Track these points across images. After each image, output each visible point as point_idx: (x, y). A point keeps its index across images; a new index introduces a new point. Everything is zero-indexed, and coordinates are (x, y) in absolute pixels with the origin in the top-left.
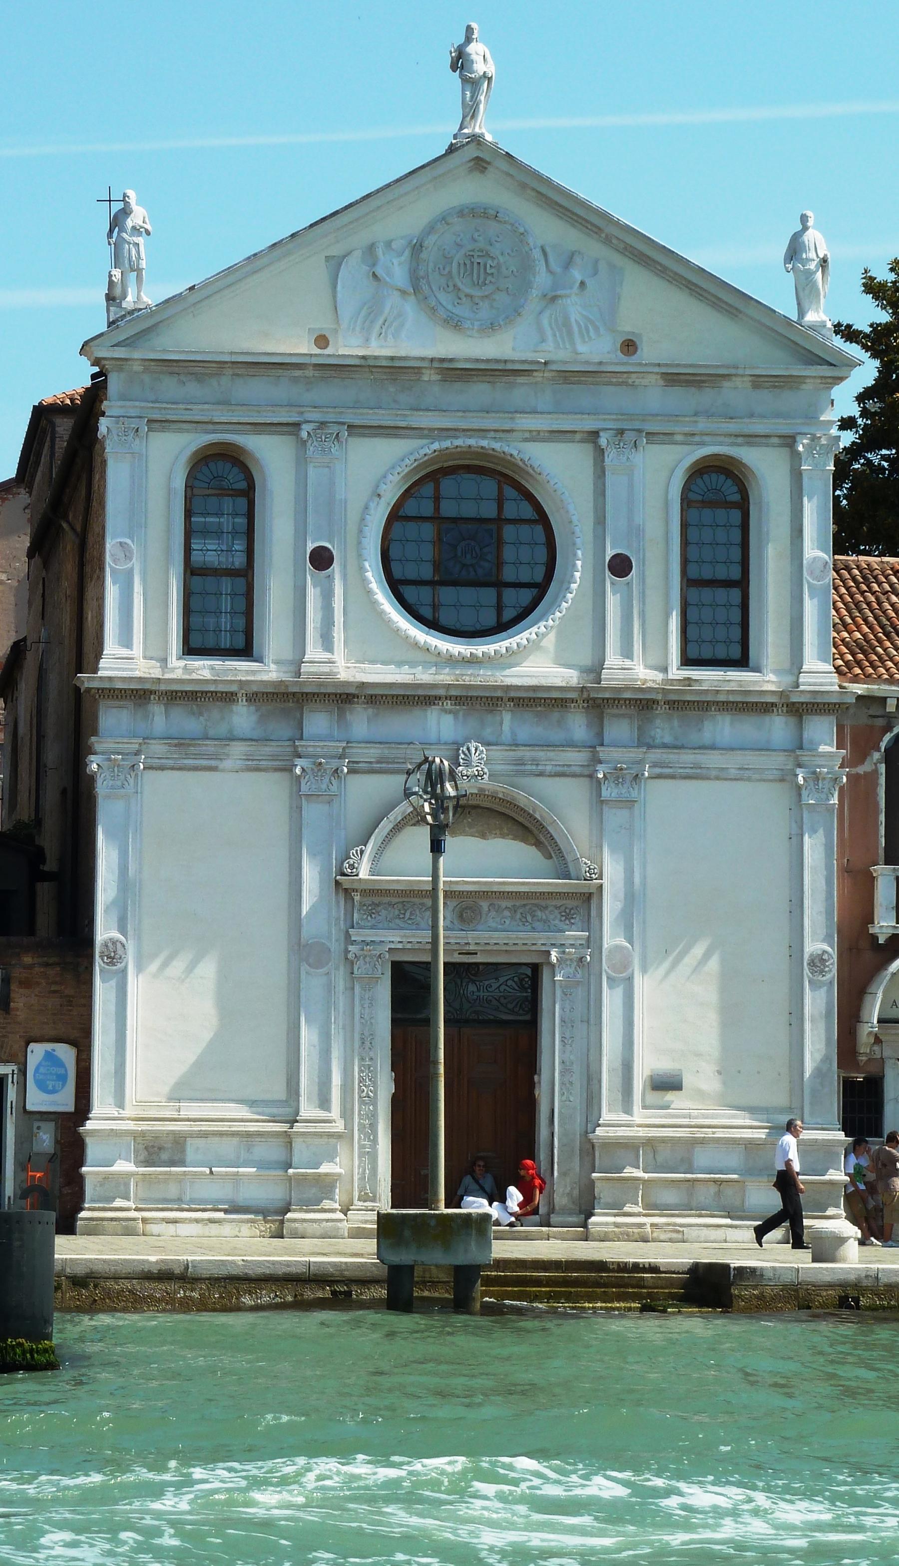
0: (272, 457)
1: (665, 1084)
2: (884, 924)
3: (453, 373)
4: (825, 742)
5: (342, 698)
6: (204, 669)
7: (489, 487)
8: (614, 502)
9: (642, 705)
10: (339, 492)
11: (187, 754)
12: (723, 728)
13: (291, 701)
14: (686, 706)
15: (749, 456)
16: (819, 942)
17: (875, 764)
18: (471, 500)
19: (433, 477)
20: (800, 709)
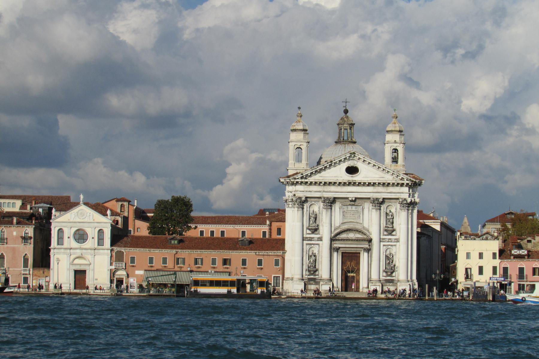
1: (97, 280)
6: (59, 246)
8: (92, 233)
12: (101, 251)
17: (114, 254)
18: (81, 232)
19: (78, 230)
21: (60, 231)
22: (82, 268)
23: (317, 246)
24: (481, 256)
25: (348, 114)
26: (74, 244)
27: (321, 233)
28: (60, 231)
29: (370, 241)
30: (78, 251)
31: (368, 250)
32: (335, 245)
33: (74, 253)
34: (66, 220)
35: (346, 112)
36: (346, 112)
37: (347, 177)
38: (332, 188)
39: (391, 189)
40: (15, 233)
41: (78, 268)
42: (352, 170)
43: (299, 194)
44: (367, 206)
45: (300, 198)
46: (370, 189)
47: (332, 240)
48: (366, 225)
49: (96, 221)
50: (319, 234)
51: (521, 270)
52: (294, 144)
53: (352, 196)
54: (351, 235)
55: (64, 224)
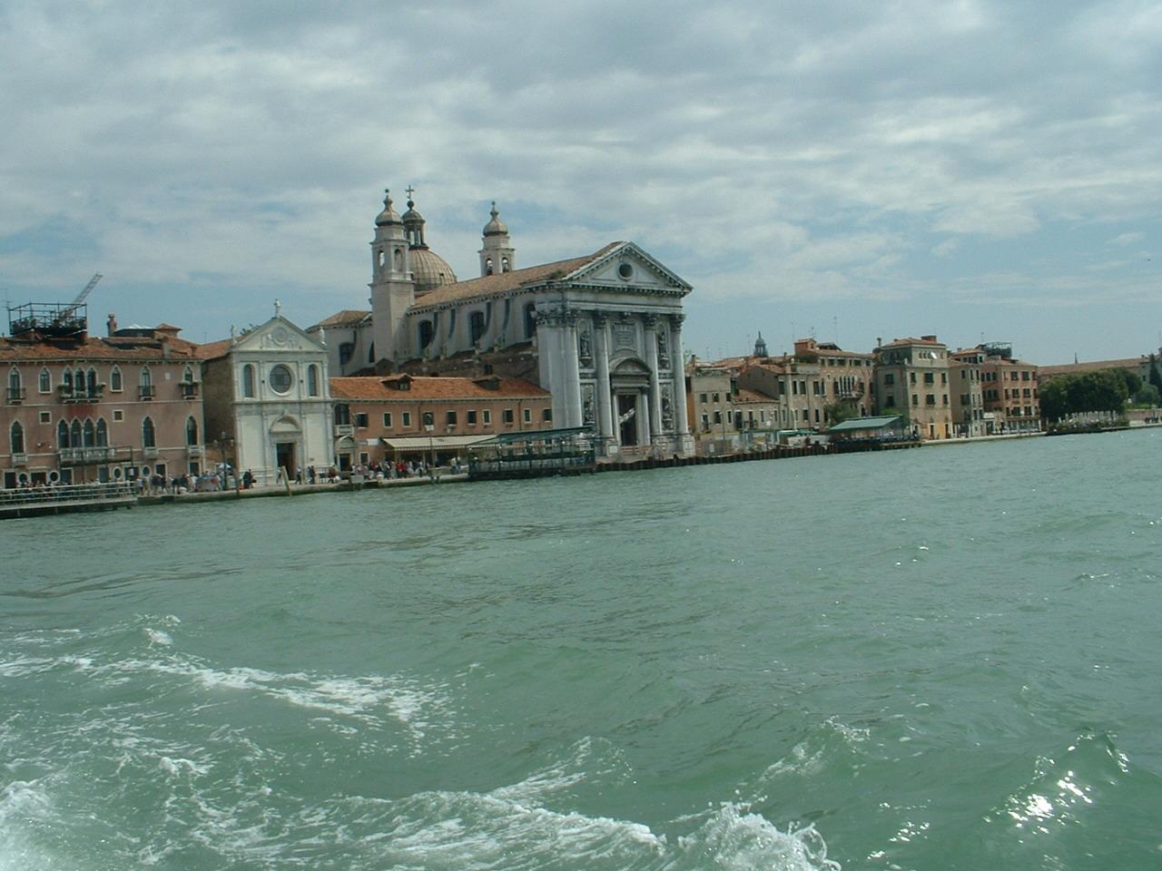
0: (254, 365)
1: (312, 460)
2: (338, 434)
3: (279, 353)
4: (329, 406)
5: (267, 403)
7: (281, 370)
8: (301, 373)
9: (305, 402)
10: (264, 372)
11: (247, 413)
12: (316, 406)
13: (261, 404)
14: (312, 403)
15: (316, 364)
16: (331, 437)
18: (280, 372)
20: (326, 402)
21: (248, 369)
22: (289, 439)
23: (591, 386)
24: (716, 399)
25: (413, 208)
26: (270, 395)
27: (595, 366)
28: (248, 369)
29: (648, 376)
30: (280, 407)
31: (649, 392)
32: (614, 385)
33: (274, 413)
34: (258, 349)
35: (410, 204)
36: (410, 204)
37: (619, 283)
38: (606, 297)
39: (665, 301)
40: (168, 376)
41: (282, 440)
42: (624, 271)
43: (570, 306)
44: (638, 326)
45: (574, 311)
46: (643, 300)
47: (611, 376)
48: (640, 355)
49: (304, 349)
50: (592, 368)
51: (751, 413)
52: (392, 243)
53: (625, 309)
54: (630, 370)
55: (253, 356)
